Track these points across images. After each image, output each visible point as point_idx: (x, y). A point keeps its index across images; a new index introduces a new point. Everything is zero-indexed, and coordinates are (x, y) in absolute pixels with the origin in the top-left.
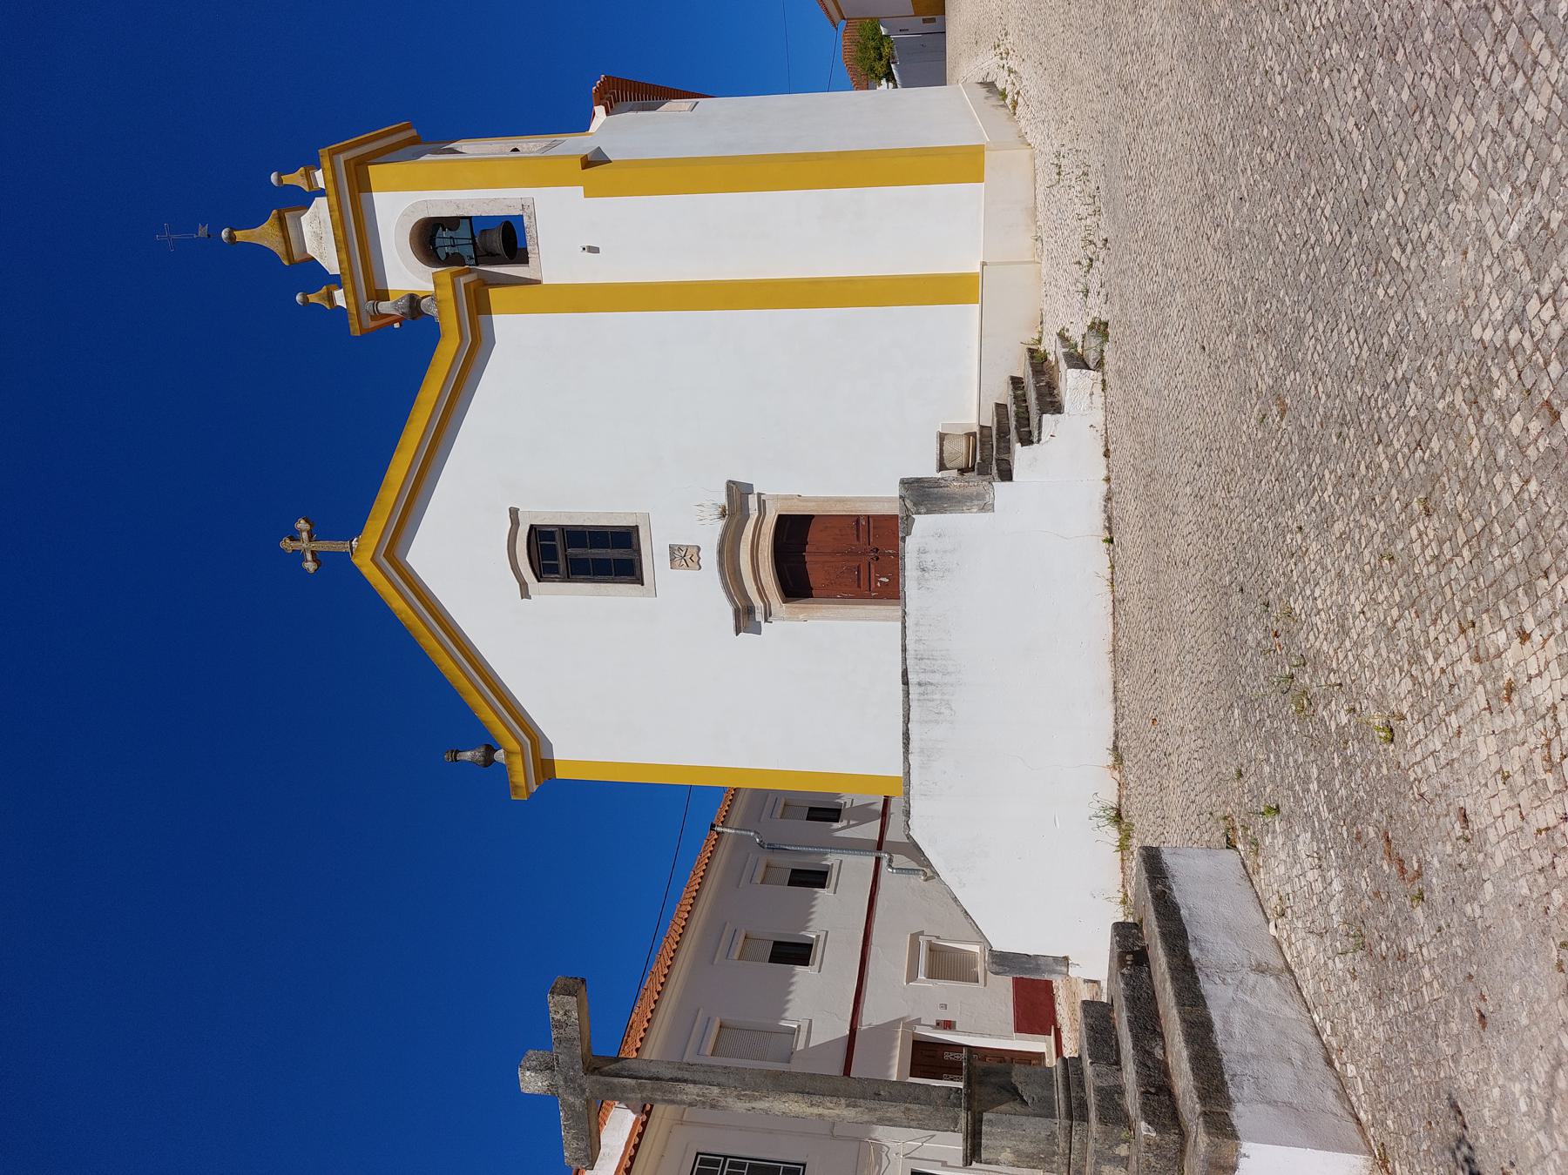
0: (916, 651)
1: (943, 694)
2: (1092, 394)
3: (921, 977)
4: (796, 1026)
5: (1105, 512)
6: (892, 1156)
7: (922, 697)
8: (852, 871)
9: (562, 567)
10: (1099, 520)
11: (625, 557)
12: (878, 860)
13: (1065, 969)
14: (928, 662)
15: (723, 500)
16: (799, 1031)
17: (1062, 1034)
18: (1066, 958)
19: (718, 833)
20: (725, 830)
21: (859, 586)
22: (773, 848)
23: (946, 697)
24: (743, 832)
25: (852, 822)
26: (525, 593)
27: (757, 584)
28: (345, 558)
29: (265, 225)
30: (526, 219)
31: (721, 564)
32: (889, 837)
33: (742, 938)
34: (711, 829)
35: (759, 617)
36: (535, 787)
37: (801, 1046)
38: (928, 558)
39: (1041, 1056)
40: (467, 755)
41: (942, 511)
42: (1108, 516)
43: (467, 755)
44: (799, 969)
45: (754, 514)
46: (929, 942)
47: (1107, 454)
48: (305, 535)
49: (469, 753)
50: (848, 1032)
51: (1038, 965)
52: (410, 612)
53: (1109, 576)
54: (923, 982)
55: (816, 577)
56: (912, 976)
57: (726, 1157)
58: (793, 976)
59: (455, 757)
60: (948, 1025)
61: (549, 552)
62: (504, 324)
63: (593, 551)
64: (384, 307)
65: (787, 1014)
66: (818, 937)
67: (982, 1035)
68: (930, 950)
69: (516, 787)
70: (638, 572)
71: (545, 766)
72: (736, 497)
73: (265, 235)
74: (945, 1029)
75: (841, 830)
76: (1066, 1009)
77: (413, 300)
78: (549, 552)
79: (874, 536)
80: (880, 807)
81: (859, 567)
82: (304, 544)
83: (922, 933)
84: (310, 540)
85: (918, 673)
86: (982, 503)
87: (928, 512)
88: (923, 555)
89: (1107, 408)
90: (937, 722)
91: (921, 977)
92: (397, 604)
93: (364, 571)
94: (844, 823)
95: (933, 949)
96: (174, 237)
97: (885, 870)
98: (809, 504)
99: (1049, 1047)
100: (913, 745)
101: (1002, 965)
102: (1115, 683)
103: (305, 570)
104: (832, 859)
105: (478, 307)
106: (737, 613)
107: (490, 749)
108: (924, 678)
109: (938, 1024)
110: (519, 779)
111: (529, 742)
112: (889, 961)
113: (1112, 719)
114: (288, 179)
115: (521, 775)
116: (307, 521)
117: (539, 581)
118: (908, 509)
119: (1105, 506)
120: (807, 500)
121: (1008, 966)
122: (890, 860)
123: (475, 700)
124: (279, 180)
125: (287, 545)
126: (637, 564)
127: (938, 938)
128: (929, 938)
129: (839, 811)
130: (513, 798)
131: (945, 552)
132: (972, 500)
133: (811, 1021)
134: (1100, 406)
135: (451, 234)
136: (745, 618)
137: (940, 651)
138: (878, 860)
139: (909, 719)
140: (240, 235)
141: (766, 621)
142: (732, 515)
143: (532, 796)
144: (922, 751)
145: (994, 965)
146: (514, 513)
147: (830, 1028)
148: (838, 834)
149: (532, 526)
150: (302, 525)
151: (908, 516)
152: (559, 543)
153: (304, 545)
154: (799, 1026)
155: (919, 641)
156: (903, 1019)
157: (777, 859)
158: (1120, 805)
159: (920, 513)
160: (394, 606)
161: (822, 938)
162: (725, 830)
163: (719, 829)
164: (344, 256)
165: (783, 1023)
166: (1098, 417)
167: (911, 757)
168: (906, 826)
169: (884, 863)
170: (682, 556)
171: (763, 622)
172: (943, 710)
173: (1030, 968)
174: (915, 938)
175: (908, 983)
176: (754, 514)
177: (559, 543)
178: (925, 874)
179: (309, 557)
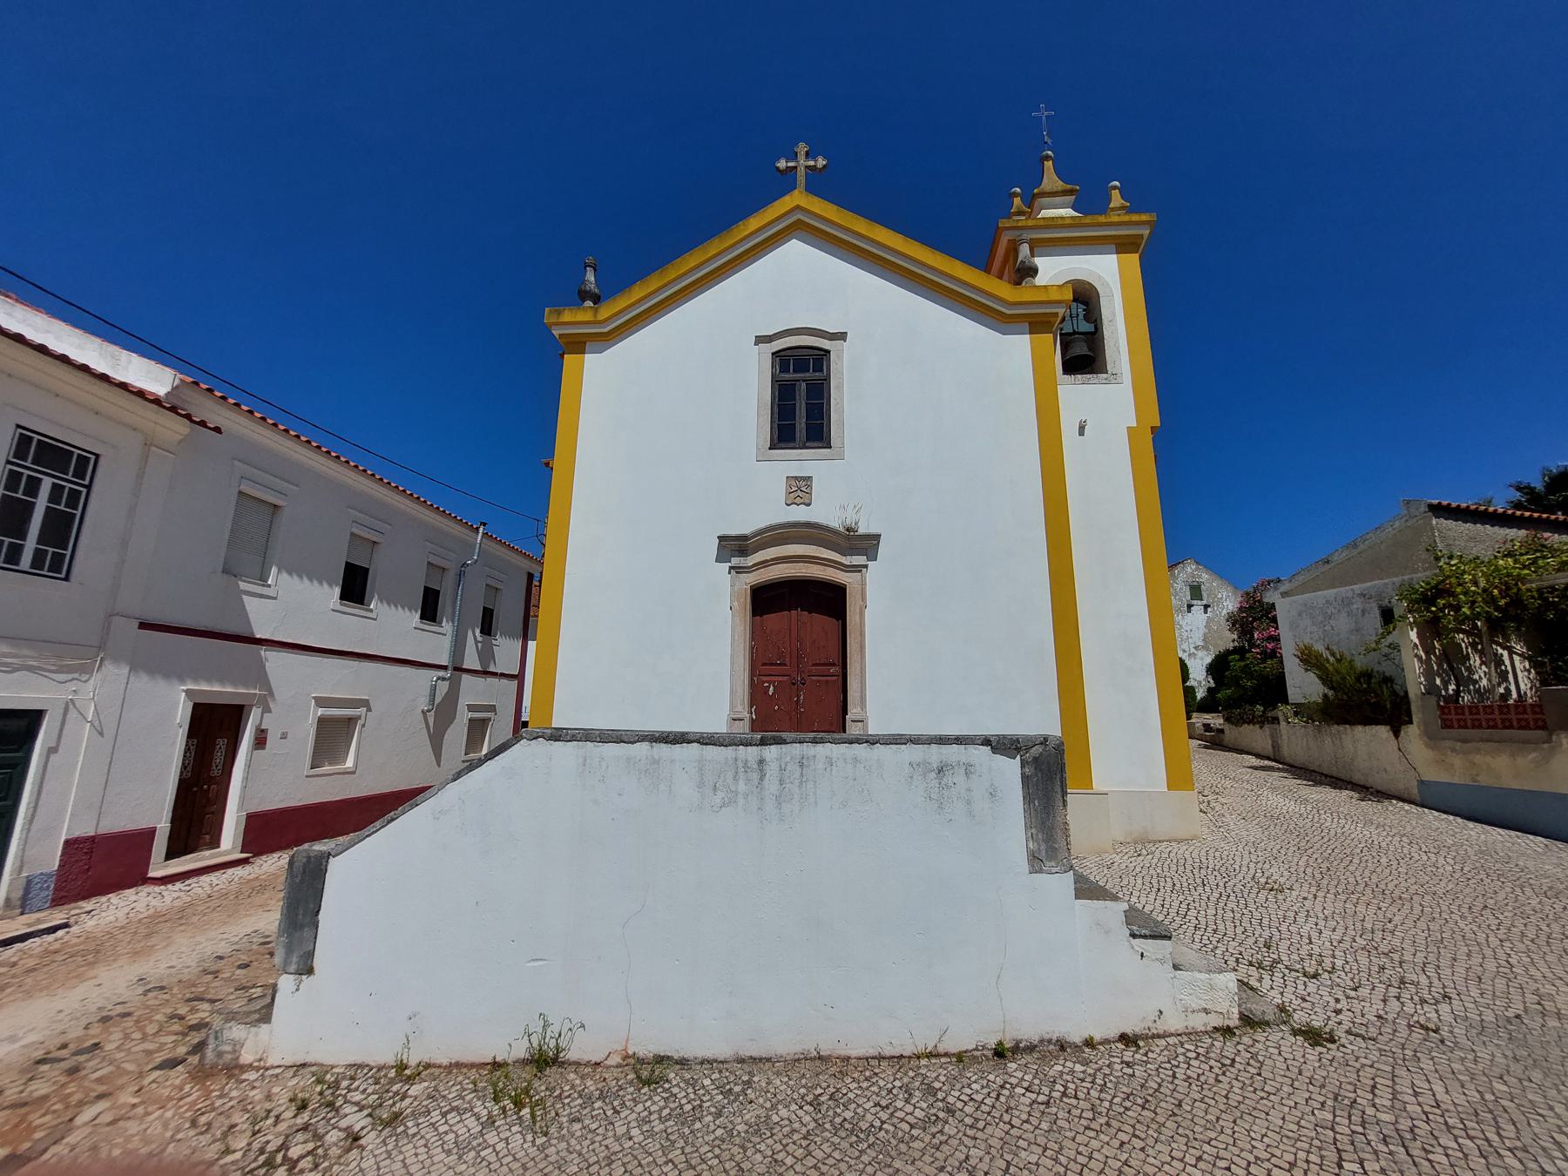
0: (815, 757)
1: (746, 796)
2: (1206, 1011)
3: (320, 712)
4: (269, 582)
5: (1042, 1041)
6: (72, 686)
7: (740, 764)
8: (435, 644)
10: (1029, 1031)
11: (798, 435)
12: (444, 668)
13: (293, 968)
14: (797, 775)
15: (861, 531)
16: (263, 585)
17: (240, 868)
19: (477, 529)
20: (480, 535)
21: (764, 664)
22: (460, 575)
24: (477, 550)
25: (480, 645)
26: (760, 340)
27: (772, 560)
28: (790, 187)
30: (1105, 376)
32: (465, 677)
33: (374, 539)
34: (481, 523)
35: (735, 561)
36: (556, 333)
37: (243, 585)
38: (960, 778)
39: (215, 843)
41: (1028, 798)
42: (1036, 1046)
44: (337, 591)
45: (846, 560)
46: (359, 717)
47: (1124, 1038)
49: (593, 279)
50: (258, 636)
51: (302, 927)
53: (941, 1049)
54: (315, 712)
55: (774, 620)
56: (320, 702)
57: (89, 487)
58: (330, 585)
59: (589, 266)
60: (260, 741)
61: (801, 365)
62: (1020, 346)
63: (804, 405)
64: (1024, 250)
65: (285, 575)
66: (371, 611)
67: (246, 779)
68: (350, 719)
69: (559, 313)
70: (782, 445)
71: (579, 345)
72: (865, 543)
73: (1051, 181)
74: (256, 739)
75: (473, 636)
76: (272, 869)
77: (1033, 271)
78: (801, 365)
79: (819, 681)
80: (492, 669)
81: (785, 665)
83: (369, 710)
84: (807, 167)
85: (779, 759)
86: (1043, 855)
87: (1025, 779)
88: (962, 771)
89: (1191, 1034)
90: (701, 785)
91: (320, 712)
92: (754, 223)
93: (787, 198)
94: (479, 639)
95: (350, 722)
96: (1044, 118)
98: (857, 618)
99: (227, 853)
100: (663, 750)
101: (304, 872)
102: (769, 1060)
104: (447, 627)
105: (1036, 324)
106: (744, 538)
107: (597, 299)
108: (772, 770)
109: (263, 731)
110: (567, 316)
111: (606, 330)
112: (338, 679)
113: (709, 1054)
114: (1116, 194)
115: (574, 318)
116: (824, 166)
117: (773, 354)
118: (1028, 749)
119: (1050, 1041)
121: (302, 881)
122: (444, 679)
123: (654, 282)
124: (1115, 188)
125: (802, 148)
126: (791, 445)
127: (363, 726)
128: (363, 718)
129: (489, 633)
131: (969, 802)
132: (1046, 841)
133: (275, 598)
134: (1191, 1024)
135: (1081, 317)
136: (733, 547)
137: (815, 794)
138: (444, 668)
139: (706, 744)
140: (1049, 164)
141: (731, 568)
142: (848, 538)
143: (547, 328)
144: (656, 762)
145: (305, 860)
146: (842, 336)
147: (263, 618)
148: (470, 633)
149: (829, 352)
150: (821, 162)
151: (1018, 750)
152: (809, 375)
153: (802, 162)
154: (269, 586)
155: (830, 762)
156: (271, 694)
157: (450, 578)
158: (563, 1063)
159: (1023, 766)
160: (751, 220)
162: (480, 535)
163: (481, 530)
164: (1068, 222)
165: (274, 570)
166: (1174, 1022)
167: (645, 746)
168: (535, 735)
169: (441, 673)
170: (800, 489)
171: (729, 564)
172: (720, 795)
173: (297, 915)
175: (314, 698)
176: (846, 560)
177: (809, 375)
178: (429, 711)
179: (791, 164)
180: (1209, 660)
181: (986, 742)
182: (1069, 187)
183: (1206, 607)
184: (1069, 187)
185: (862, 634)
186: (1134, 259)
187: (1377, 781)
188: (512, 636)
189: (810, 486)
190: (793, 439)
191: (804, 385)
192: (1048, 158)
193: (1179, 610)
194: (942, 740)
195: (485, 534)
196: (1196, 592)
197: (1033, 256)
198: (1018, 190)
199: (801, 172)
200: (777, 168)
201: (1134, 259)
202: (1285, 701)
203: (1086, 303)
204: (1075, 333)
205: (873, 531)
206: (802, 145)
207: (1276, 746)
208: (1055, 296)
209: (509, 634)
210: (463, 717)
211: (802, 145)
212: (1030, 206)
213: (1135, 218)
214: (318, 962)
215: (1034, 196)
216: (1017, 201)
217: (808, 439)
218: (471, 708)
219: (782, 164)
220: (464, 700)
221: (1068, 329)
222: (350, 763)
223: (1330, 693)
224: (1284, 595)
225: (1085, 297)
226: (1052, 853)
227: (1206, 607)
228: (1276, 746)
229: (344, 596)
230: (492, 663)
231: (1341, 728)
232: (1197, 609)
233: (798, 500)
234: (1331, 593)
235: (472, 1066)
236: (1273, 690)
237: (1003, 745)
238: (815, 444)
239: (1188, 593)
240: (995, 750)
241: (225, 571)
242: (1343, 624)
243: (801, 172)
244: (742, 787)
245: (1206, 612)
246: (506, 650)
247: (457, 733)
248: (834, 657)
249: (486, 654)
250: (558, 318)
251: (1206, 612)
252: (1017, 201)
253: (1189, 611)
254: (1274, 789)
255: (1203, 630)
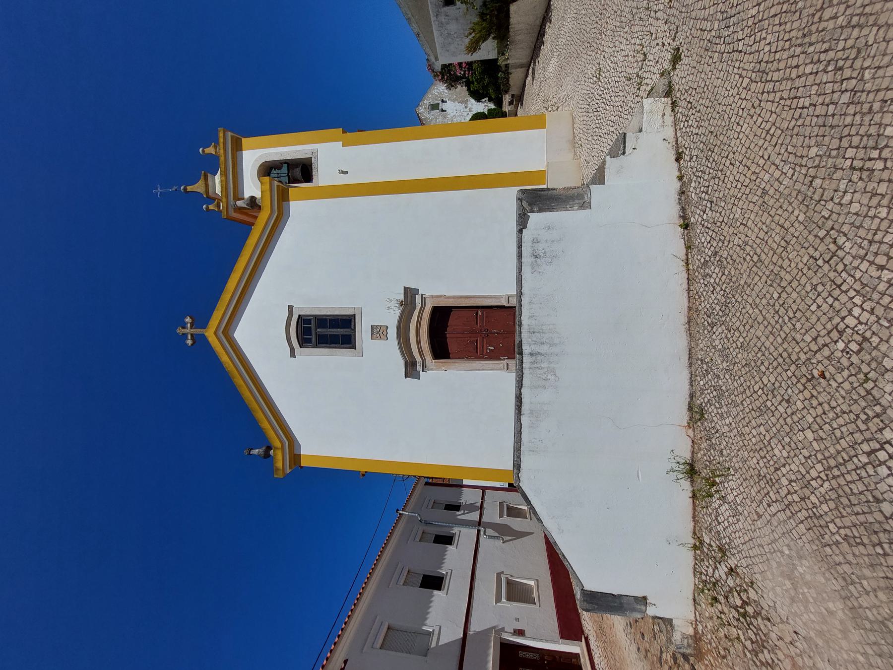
0: (529, 325)
1: (550, 363)
2: (664, 115)
3: (504, 600)
4: (431, 630)
5: (680, 204)
7: (533, 366)
8: (465, 536)
9: (314, 339)
10: (673, 211)
11: (347, 333)
12: (479, 531)
13: (643, 608)
14: (538, 335)
15: (402, 297)
16: (433, 634)
17: (590, 642)
18: (645, 598)
19: (400, 514)
20: (404, 513)
21: (477, 352)
22: (426, 523)
23: (552, 365)
24: (412, 514)
25: (466, 512)
26: (293, 354)
27: (418, 348)
28: (204, 338)
29: (200, 182)
30: (313, 159)
31: (398, 334)
32: (484, 519)
33: (406, 572)
35: (419, 368)
36: (289, 471)
37: (433, 645)
38: (540, 246)
39: (577, 656)
40: (255, 452)
41: (551, 209)
42: (682, 207)
43: (255, 452)
44: (436, 592)
45: (419, 306)
46: (507, 578)
47: (678, 159)
48: (189, 325)
49: (257, 450)
50: (462, 636)
51: (621, 603)
52: (230, 363)
53: (684, 258)
54: (504, 603)
55: (452, 347)
56: (498, 600)
58: (432, 596)
59: (250, 452)
60: (520, 633)
61: (307, 331)
62: (296, 207)
63: (330, 330)
64: (240, 203)
65: (427, 622)
66: (447, 573)
67: (541, 640)
68: (507, 583)
69: (277, 469)
70: (353, 342)
71: (296, 458)
72: (409, 295)
73: (199, 187)
74: (519, 635)
75: (461, 515)
76: (591, 624)
77: (253, 199)
78: (307, 331)
79: (486, 321)
80: (479, 505)
81: (477, 340)
82: (188, 330)
83: (502, 573)
84: (191, 328)
85: (530, 345)
86: (581, 202)
88: (535, 244)
89: (675, 124)
90: (544, 387)
91: (504, 600)
92: (224, 358)
93: (210, 339)
94: (462, 512)
95: (509, 583)
96: (161, 191)
97: (482, 537)
98: (450, 300)
99: (582, 650)
100: (525, 408)
101: (592, 603)
102: (690, 350)
103: (187, 344)
104: (456, 530)
105: (284, 197)
107: (269, 448)
108: (536, 348)
109: (514, 632)
110: (279, 465)
111: (287, 442)
112: (486, 590)
113: (687, 382)
114: (207, 150)
115: (280, 460)
116: (191, 318)
117: (301, 347)
118: (524, 209)
119: (680, 199)
120: (449, 297)
121: (597, 604)
122: (485, 531)
123: (259, 415)
124: (203, 151)
125: (180, 331)
126: (353, 337)
127: (511, 576)
128: (507, 576)
129: (460, 506)
130: (275, 476)
131: (553, 241)
132: (574, 200)
133: (440, 627)
134: (670, 124)
135: (279, 172)
136: (411, 369)
137: (549, 325)
138: (479, 531)
139: (522, 384)
140: (189, 188)
141: (423, 371)
142: (406, 305)
144: (532, 412)
145: (585, 603)
146: (291, 308)
147: (452, 633)
148: (459, 517)
149: (300, 316)
150: (188, 320)
151: (525, 214)
152: (313, 326)
153: (188, 331)
154: (433, 630)
156: (494, 627)
158: (692, 460)
159: (533, 212)
161: (449, 574)
162: (404, 513)
163: (401, 512)
164: (223, 178)
165: (424, 628)
166: (669, 132)
167: (523, 418)
168: (517, 478)
169: (482, 533)
170: (378, 332)
171: (421, 372)
173: (615, 606)
174: (499, 575)
175: (496, 604)
176: (419, 306)
177: (313, 326)
178: (503, 539)
179: (189, 337)
180: (473, 101)
181: (520, 231)
182: (202, 177)
183: (443, 101)
184: (202, 177)
185: (461, 297)
186: (245, 141)
187: (540, 12)
188: (460, 494)
189: (377, 326)
190: (350, 336)
191: (318, 330)
192: (185, 189)
193: (445, 117)
194: (520, 256)
195: (403, 510)
196: (434, 107)
197: (243, 199)
198: (204, 206)
199: (194, 331)
200: (192, 345)
201: (245, 141)
202: (496, 60)
203: (271, 168)
204: (288, 175)
205: (402, 291)
206: (178, 331)
207: (521, 66)
208: (267, 187)
209: (460, 494)
210: (506, 520)
211: (178, 331)
212: (214, 199)
213: (221, 140)
214: (640, 595)
215: (208, 197)
216: (211, 207)
217: (350, 327)
218: (501, 516)
219: (189, 342)
220: (497, 520)
221: (286, 179)
222: (532, 583)
223: (492, 35)
224: (437, 59)
225: (267, 169)
226: (580, 196)
227: (443, 101)
228: (521, 66)
229: (439, 588)
230: (476, 504)
231: (511, 30)
232: (444, 106)
233: (385, 333)
234: (436, 34)
235: (694, 509)
236: (490, 66)
237: (522, 222)
238: (353, 323)
239: (435, 111)
240: (525, 227)
241: (426, 655)
242: (453, 27)
243: (194, 331)
244: (545, 365)
245: (446, 102)
246: (469, 497)
247: (515, 523)
248: (473, 313)
249: (471, 508)
250: (280, 470)
251: (446, 102)
252: (211, 207)
253: (445, 111)
254: (545, 69)
255: (456, 104)
